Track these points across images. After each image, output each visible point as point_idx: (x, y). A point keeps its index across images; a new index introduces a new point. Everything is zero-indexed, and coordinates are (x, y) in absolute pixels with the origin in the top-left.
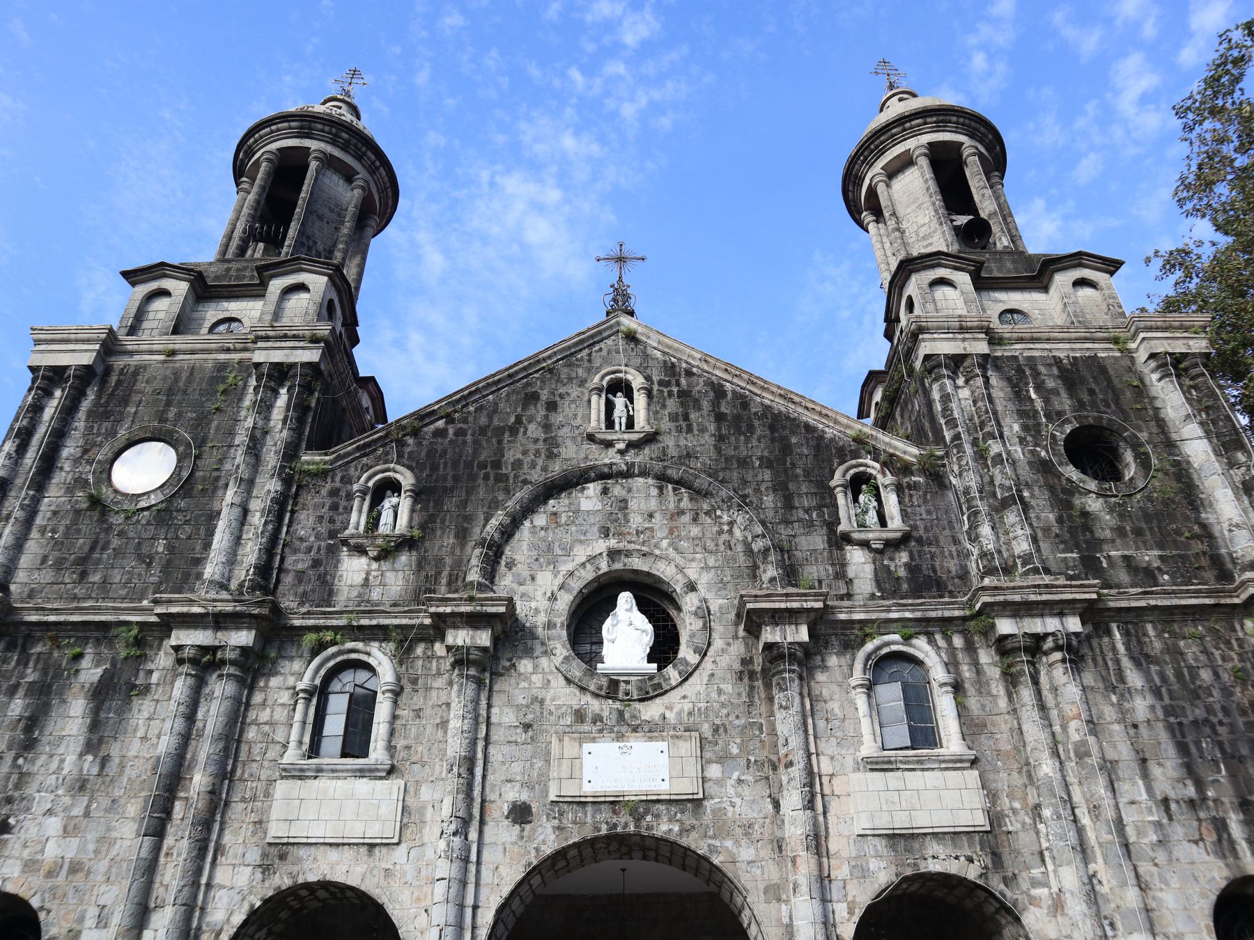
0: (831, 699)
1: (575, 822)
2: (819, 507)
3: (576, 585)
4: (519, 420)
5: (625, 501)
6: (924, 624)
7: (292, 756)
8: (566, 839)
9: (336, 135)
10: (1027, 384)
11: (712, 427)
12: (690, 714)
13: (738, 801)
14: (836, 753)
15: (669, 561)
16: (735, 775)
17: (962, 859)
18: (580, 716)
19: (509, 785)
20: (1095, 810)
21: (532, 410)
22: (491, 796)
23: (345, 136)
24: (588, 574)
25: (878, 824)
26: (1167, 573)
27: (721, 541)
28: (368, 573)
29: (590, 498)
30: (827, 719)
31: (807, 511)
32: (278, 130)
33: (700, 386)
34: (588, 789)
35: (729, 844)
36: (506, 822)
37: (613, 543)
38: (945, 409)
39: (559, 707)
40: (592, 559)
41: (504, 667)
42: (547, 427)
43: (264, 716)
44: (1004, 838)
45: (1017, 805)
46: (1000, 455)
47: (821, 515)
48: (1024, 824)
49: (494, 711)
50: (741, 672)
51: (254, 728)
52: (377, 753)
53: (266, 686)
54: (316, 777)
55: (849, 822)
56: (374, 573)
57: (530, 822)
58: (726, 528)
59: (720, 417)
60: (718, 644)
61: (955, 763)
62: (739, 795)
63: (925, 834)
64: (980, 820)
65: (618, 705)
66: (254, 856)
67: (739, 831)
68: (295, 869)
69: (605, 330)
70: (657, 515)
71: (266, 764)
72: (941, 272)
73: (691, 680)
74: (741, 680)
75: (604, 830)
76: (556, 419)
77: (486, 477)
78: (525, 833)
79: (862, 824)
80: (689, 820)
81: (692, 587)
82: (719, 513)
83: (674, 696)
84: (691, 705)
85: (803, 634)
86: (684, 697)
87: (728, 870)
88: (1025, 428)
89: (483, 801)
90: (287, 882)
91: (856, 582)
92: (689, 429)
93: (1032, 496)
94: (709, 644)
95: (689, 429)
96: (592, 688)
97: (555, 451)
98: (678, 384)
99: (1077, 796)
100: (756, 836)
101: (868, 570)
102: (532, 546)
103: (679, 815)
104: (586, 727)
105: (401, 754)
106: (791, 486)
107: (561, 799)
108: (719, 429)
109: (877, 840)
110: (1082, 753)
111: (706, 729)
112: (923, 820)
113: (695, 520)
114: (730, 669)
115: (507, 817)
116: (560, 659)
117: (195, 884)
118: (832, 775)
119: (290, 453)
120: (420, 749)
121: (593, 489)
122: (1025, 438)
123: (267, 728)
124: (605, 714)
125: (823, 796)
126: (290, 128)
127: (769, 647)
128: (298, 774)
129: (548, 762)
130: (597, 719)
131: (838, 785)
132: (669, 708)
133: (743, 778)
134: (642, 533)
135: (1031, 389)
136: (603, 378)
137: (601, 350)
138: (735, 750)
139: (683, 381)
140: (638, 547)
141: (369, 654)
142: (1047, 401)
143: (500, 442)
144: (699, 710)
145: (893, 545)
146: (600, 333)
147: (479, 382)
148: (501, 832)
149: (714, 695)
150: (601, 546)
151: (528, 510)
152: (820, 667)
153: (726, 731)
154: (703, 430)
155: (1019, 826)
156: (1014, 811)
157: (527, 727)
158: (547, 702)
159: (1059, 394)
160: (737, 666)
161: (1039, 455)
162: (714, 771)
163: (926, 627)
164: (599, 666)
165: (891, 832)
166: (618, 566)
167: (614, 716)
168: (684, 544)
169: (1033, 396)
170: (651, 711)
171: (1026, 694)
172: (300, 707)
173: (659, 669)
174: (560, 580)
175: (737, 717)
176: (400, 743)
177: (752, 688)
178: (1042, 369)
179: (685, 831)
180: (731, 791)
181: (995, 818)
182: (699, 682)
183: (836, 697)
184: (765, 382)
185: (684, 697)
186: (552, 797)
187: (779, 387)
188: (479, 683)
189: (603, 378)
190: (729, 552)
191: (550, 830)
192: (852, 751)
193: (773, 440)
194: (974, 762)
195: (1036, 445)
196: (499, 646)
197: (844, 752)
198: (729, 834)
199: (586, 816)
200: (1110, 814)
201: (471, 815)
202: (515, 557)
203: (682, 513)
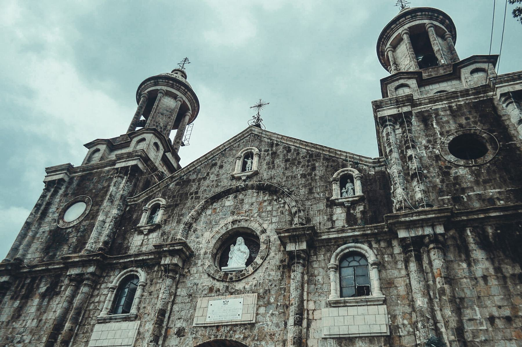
0: (318, 275)
1: (201, 335)
2: (324, 192)
3: (218, 236)
6: (366, 237)
7: (103, 314)
8: (197, 343)
9: (168, 82)
11: (283, 165)
12: (255, 286)
14: (317, 299)
15: (256, 221)
18: (211, 290)
19: (179, 320)
20: (446, 324)
21: (213, 170)
22: (171, 325)
23: (171, 82)
24: (223, 231)
25: (332, 333)
26: (502, 200)
27: (279, 211)
28: (143, 241)
29: (229, 202)
30: (315, 285)
31: (318, 194)
32: (147, 85)
34: (208, 320)
36: (175, 336)
37: (235, 217)
39: (203, 286)
41: (186, 272)
43: (97, 300)
44: (397, 339)
45: (406, 322)
46: (411, 155)
48: (409, 332)
49: (179, 290)
50: (280, 266)
51: (93, 304)
52: (133, 311)
53: (100, 288)
54: (109, 322)
55: (319, 332)
56: (145, 240)
57: (183, 336)
59: (287, 161)
60: (272, 254)
61: (375, 302)
63: (356, 337)
64: (384, 329)
65: (227, 284)
67: (268, 337)
69: (245, 134)
70: (255, 204)
71: (94, 318)
72: (402, 81)
73: (258, 271)
74: (279, 269)
75: (213, 338)
78: (182, 341)
79: (325, 332)
80: (247, 332)
81: (264, 231)
83: (250, 279)
84: (256, 282)
85: (304, 246)
86: (254, 279)
88: (429, 141)
91: (336, 222)
93: (429, 172)
94: (268, 255)
96: (217, 278)
97: (219, 184)
98: (272, 150)
99: (439, 317)
100: (275, 339)
101: (344, 216)
103: (244, 330)
104: (213, 295)
105: (141, 311)
106: (313, 184)
107: (198, 326)
109: (332, 340)
110: (442, 292)
111: (261, 291)
112: (354, 330)
114: (275, 265)
115: (176, 334)
116: (207, 267)
118: (314, 310)
120: (148, 308)
121: (231, 197)
122: (428, 146)
123: (97, 304)
124: (221, 288)
125: (308, 319)
126: (151, 83)
127: (290, 253)
128: (104, 321)
129: (195, 310)
131: (317, 315)
132: (248, 284)
133: (274, 313)
134: (248, 212)
136: (242, 153)
137: (244, 142)
140: (245, 218)
141: (137, 272)
143: (199, 184)
144: (259, 283)
145: (354, 204)
146: (243, 135)
147: (194, 162)
149: (267, 277)
150: (230, 219)
151: (204, 208)
152: (315, 261)
153: (270, 292)
154: (279, 166)
155: (406, 333)
156: (404, 325)
157: (191, 295)
158: (199, 285)
159: (449, 122)
160: (278, 263)
161: (435, 153)
162: (262, 310)
163: (367, 238)
165: (338, 336)
166: (236, 226)
167: (224, 289)
169: (435, 126)
170: (239, 286)
171: (413, 266)
172: (109, 295)
174: (213, 234)
175: (275, 286)
177: (283, 272)
179: (245, 338)
180: (268, 319)
181: (394, 328)
182: (261, 271)
183: (321, 274)
184: (306, 142)
185: (254, 279)
186: (194, 325)
187: (312, 144)
188: (174, 278)
189: (242, 153)
190: (282, 215)
191: (191, 339)
192: (325, 298)
194: (385, 302)
195: (433, 148)
196: (185, 264)
197: (321, 299)
199: (206, 333)
200: (453, 324)
201: (161, 334)
202: (197, 227)
203: (265, 201)
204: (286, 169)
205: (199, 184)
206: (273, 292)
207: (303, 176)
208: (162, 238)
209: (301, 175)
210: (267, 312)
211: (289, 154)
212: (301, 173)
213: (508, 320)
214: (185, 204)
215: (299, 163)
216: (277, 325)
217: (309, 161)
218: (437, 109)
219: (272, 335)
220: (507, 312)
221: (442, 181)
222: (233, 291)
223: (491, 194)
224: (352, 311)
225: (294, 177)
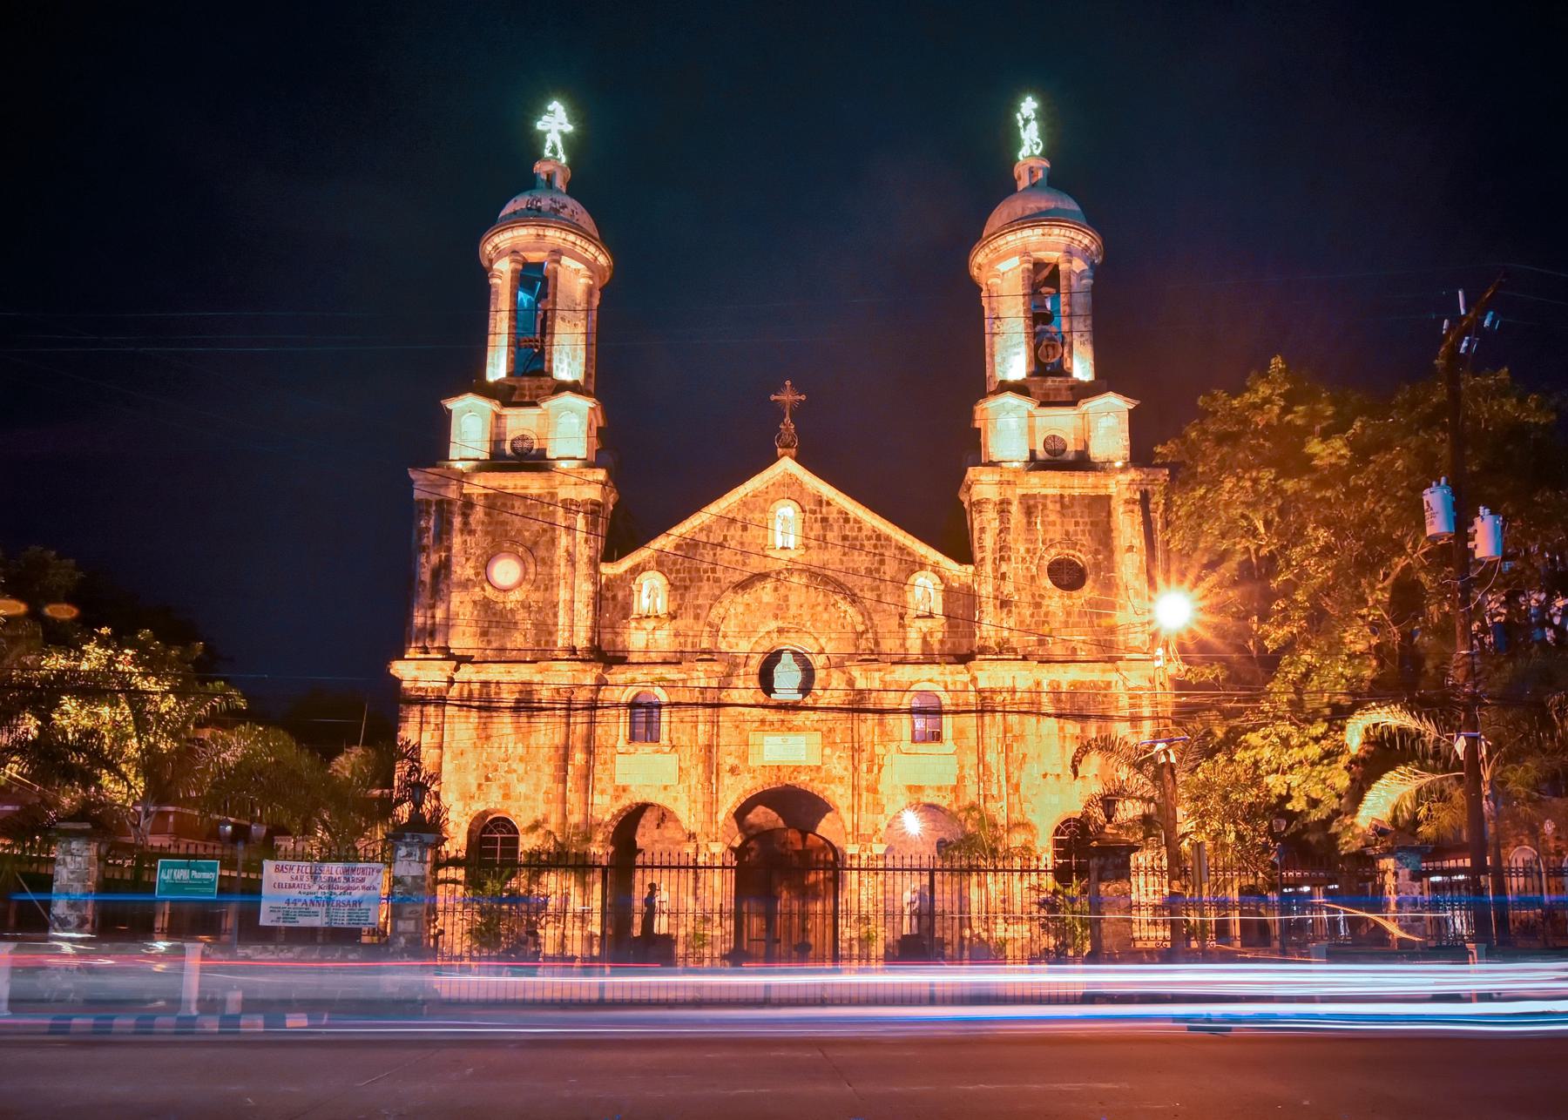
5: (787, 596)
7: (621, 744)
13: (838, 766)
16: (838, 753)
18: (763, 722)
21: (732, 532)
28: (648, 641)
33: (833, 516)
35: (832, 786)
36: (729, 774)
37: (780, 624)
38: (980, 538)
42: (742, 544)
58: (842, 615)
62: (839, 763)
66: (610, 791)
68: (631, 796)
70: (805, 606)
76: (748, 537)
77: (708, 579)
80: (814, 775)
82: (839, 605)
87: (832, 798)
88: (1028, 551)
89: (718, 764)
90: (627, 803)
98: (821, 512)
104: (766, 728)
113: (826, 609)
117: (587, 804)
119: (594, 564)
121: (769, 584)
130: (772, 723)
138: (838, 741)
139: (824, 510)
142: (1046, 532)
143: (715, 555)
148: (727, 780)
150: (773, 625)
162: (828, 751)
164: (772, 695)
168: (819, 624)
169: (1039, 526)
173: (804, 697)
176: (674, 736)
180: (835, 761)
198: (832, 782)
203: (819, 604)
204: (845, 554)
205: (715, 555)
206: (838, 732)
208: (677, 641)
209: (866, 569)
210: (833, 753)
211: (847, 526)
212: (866, 565)
214: (700, 588)
215: (862, 546)
216: (846, 769)
217: (875, 547)
218: (1045, 497)
219: (841, 779)
221: (1032, 615)
222: (790, 726)
225: (855, 572)
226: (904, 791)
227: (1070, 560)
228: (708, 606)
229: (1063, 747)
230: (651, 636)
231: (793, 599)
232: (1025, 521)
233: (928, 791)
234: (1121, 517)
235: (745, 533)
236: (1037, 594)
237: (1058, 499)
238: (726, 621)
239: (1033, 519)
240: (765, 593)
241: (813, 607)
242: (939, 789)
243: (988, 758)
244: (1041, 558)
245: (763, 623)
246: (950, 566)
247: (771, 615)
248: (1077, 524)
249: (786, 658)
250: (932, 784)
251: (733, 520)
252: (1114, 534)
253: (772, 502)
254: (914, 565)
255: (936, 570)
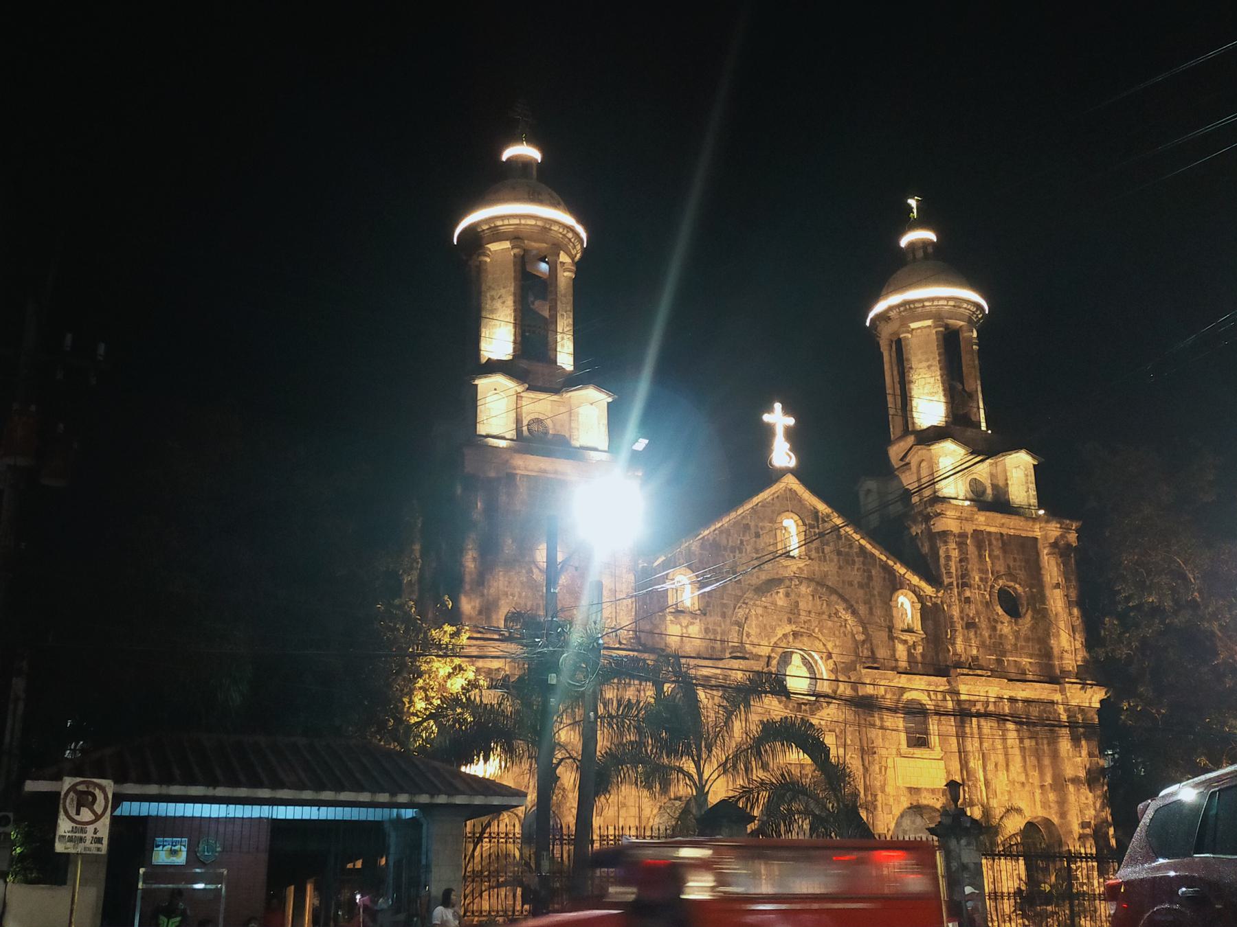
4: (742, 542)
5: (797, 602)
10: (985, 551)
17: (935, 799)
27: (841, 631)
37: (794, 627)
40: (785, 635)
47: (885, 621)
59: (839, 553)
76: (761, 543)
88: (981, 579)
92: (825, 560)
95: (825, 560)
102: (758, 626)
106: (873, 601)
108: (839, 561)
112: (923, 783)
113: (830, 616)
135: (987, 555)
137: (778, 497)
150: (788, 629)
154: (831, 561)
169: (987, 559)
178: (994, 542)
193: (864, 571)
195: (985, 591)
203: (823, 613)
207: (861, 586)
209: (859, 582)
213: (1023, 784)
218: (989, 533)
220: (1023, 779)
221: (990, 637)
223: (1024, 663)
224: (920, 763)
225: (851, 584)
226: (906, 792)
227: (1006, 590)
228: (732, 605)
229: (1024, 758)
230: (684, 631)
231: (802, 605)
232: (977, 553)
233: (924, 794)
234: (1046, 558)
235: (758, 540)
236: (992, 618)
237: (999, 536)
238: (748, 622)
239: (983, 552)
240: (780, 599)
241: (820, 614)
242: (933, 791)
243: (971, 764)
244: (992, 587)
245: (779, 625)
246: (928, 590)
247: (785, 618)
248: (1015, 560)
249: (796, 659)
250: (927, 787)
251: (747, 527)
252: (1043, 572)
253: (779, 514)
254: (895, 584)
255: (915, 591)
